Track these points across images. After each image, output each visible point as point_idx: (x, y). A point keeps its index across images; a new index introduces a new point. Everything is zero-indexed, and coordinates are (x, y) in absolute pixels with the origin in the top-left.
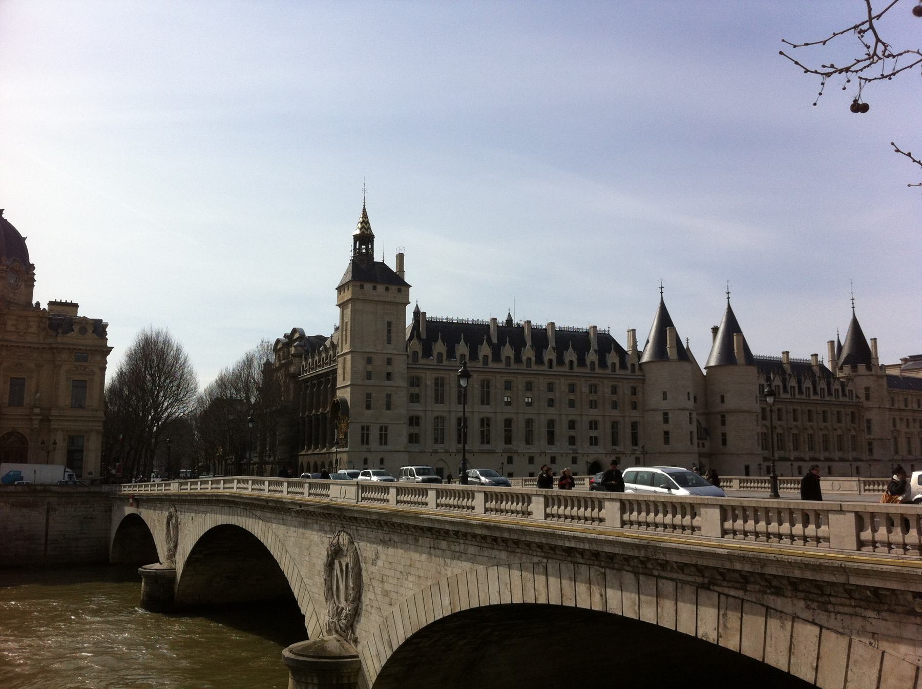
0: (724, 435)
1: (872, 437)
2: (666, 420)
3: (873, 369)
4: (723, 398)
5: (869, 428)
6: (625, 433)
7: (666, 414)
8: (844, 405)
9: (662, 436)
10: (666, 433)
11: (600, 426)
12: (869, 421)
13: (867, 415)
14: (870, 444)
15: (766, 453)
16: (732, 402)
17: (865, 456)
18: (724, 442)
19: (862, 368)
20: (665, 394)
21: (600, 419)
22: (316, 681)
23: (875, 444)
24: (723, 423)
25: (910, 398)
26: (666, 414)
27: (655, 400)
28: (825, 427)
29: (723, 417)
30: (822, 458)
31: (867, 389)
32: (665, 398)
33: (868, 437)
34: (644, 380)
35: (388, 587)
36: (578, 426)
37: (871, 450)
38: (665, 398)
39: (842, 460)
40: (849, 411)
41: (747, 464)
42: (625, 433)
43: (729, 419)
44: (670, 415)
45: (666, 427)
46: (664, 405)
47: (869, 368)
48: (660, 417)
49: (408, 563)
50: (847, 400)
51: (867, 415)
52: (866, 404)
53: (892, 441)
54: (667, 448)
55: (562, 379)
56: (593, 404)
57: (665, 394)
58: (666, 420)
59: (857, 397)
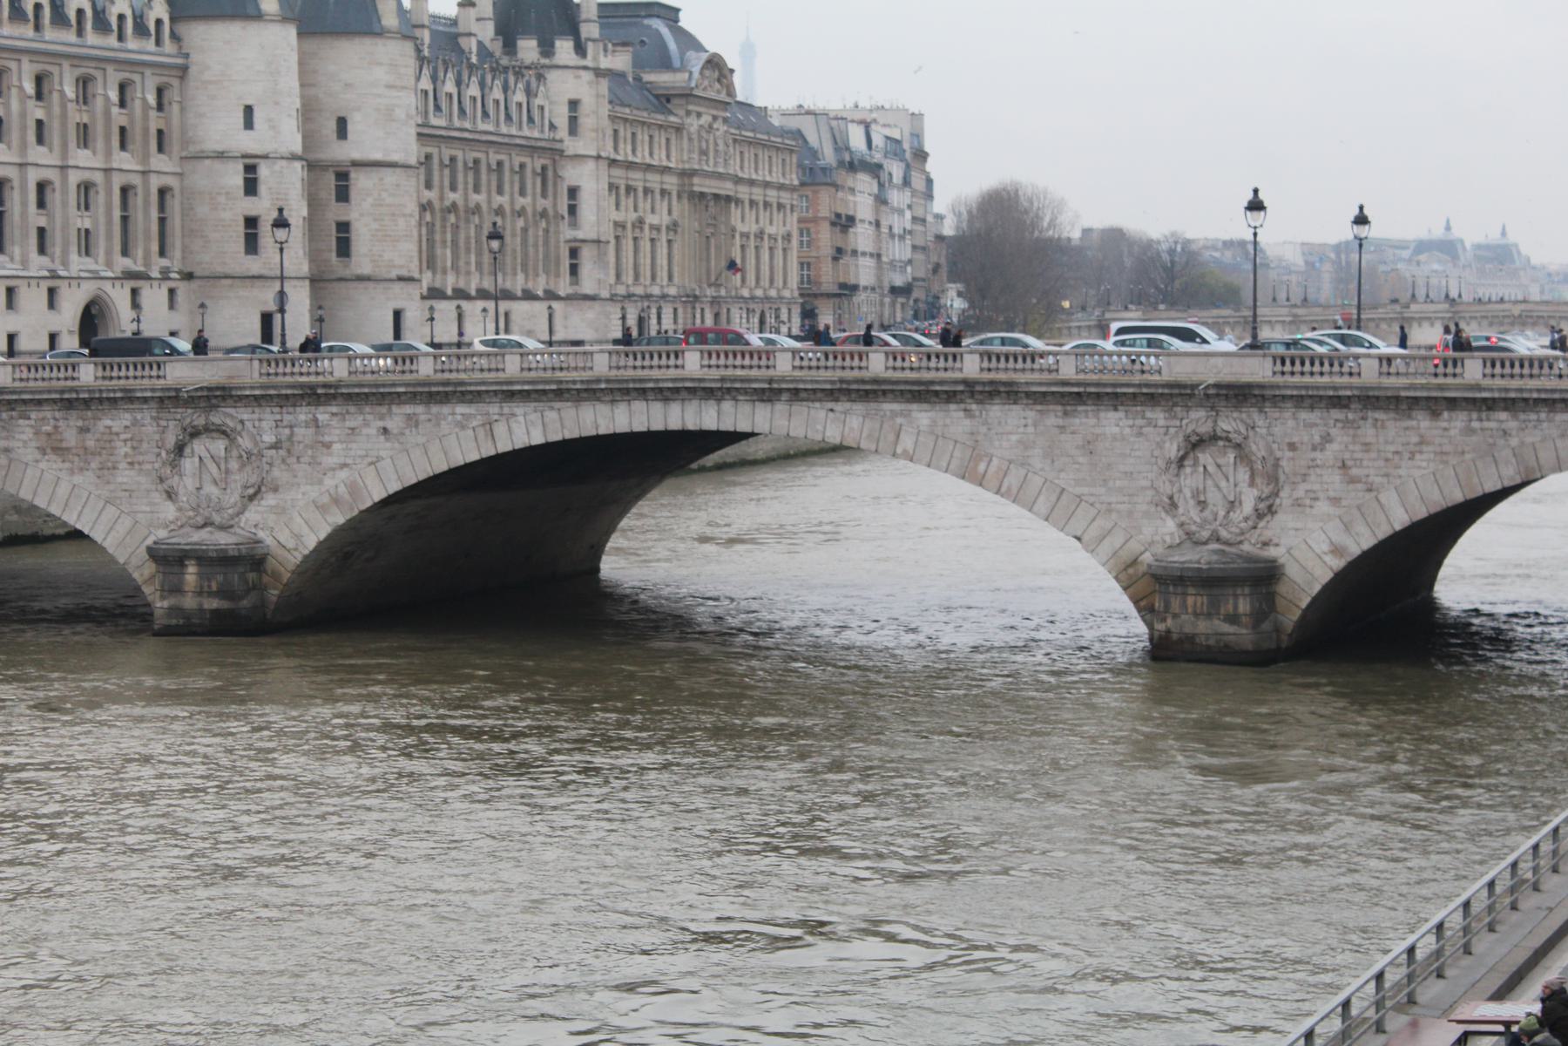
0: (344, 227)
1: (580, 235)
2: (251, 187)
3: (590, 46)
4: (342, 124)
5: (572, 210)
6: (146, 218)
7: (250, 169)
8: (532, 149)
9: (241, 228)
10: (251, 222)
11: (99, 199)
12: (573, 192)
13: (573, 174)
14: (574, 253)
15: (427, 279)
16: (366, 142)
17: (564, 287)
18: (344, 247)
19: (564, 49)
20: (249, 111)
21: (98, 177)
22: (1247, 590)
23: (586, 253)
24: (343, 195)
25: (621, 133)
26: (250, 169)
27: (219, 128)
28: (478, 207)
29: (343, 176)
30: (540, 293)
31: (574, 104)
32: (249, 124)
33: (568, 233)
34: (183, 71)
35: (1354, 471)
36: (54, 198)
37: (574, 270)
38: (249, 124)
39: (529, 296)
40: (539, 163)
41: (398, 305)
42: (146, 218)
43: (361, 182)
44: (264, 171)
45: (251, 206)
46: (249, 142)
47: (580, 50)
48: (237, 180)
49: (1415, 439)
50: (536, 134)
51: (573, 174)
52: (572, 146)
53: (613, 241)
54: (253, 265)
55: (25, 60)
56: (85, 136)
57: (249, 111)
58: (251, 187)
59: (552, 127)
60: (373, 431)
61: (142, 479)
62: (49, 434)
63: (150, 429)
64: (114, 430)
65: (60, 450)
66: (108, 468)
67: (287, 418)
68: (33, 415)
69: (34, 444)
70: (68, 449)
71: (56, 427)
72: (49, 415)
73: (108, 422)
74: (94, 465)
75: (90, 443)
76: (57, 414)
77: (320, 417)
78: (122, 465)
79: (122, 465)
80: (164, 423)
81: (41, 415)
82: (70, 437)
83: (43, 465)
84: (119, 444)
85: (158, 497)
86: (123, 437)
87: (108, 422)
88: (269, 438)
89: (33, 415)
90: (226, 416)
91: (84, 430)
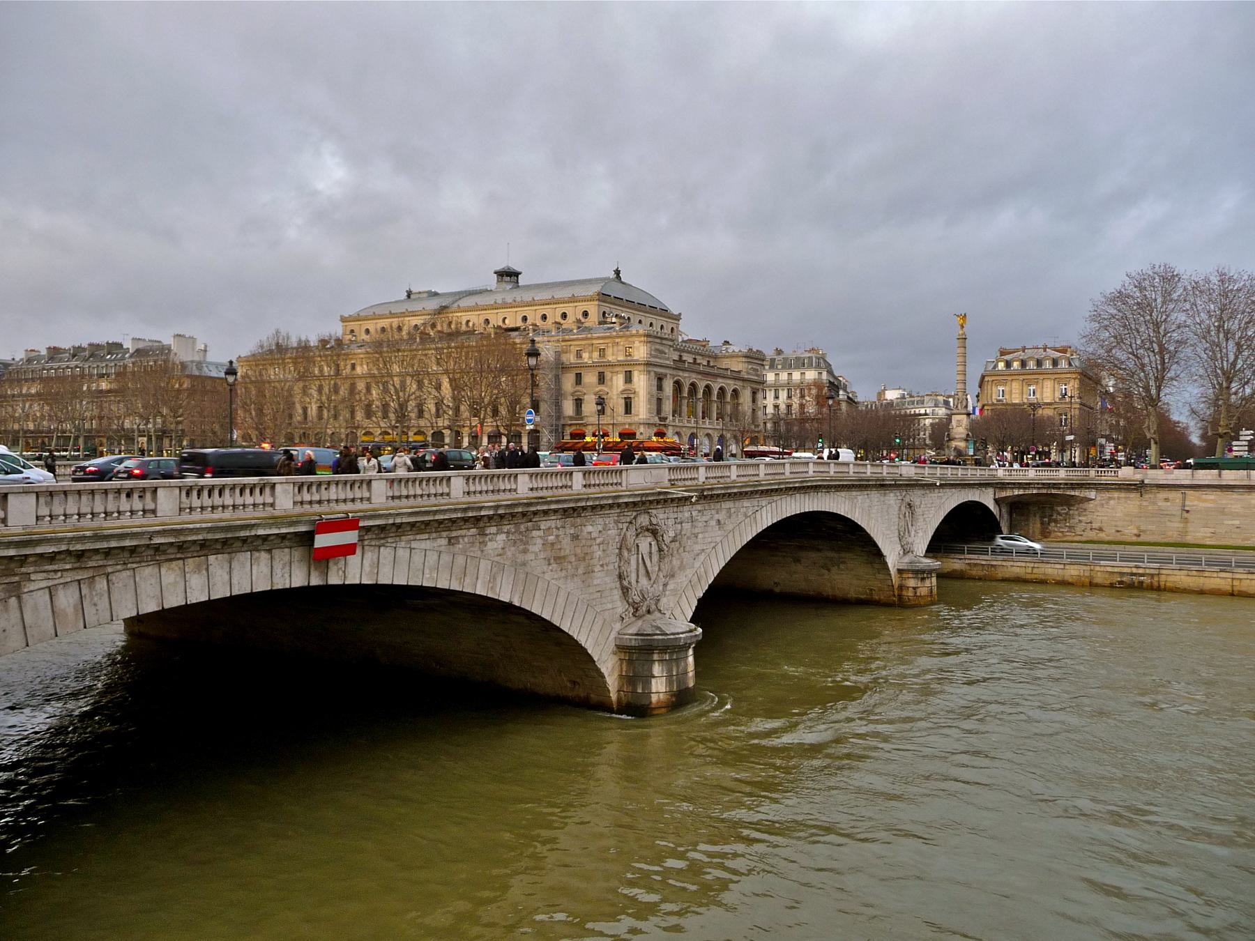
60: (713, 523)
61: (607, 579)
62: (552, 544)
63: (613, 532)
64: (594, 535)
65: (559, 559)
66: (589, 572)
67: (680, 515)
68: (543, 525)
69: (542, 555)
70: (564, 557)
71: (557, 536)
72: (552, 524)
73: (590, 528)
74: (580, 571)
75: (578, 550)
76: (559, 523)
77: (694, 514)
78: (598, 568)
79: (598, 568)
80: (620, 526)
81: (548, 524)
82: (567, 545)
83: (547, 577)
84: (596, 547)
85: (617, 594)
86: (598, 541)
87: (590, 528)
88: (672, 534)
89: (543, 525)
90: (661, 516)
91: (575, 537)
